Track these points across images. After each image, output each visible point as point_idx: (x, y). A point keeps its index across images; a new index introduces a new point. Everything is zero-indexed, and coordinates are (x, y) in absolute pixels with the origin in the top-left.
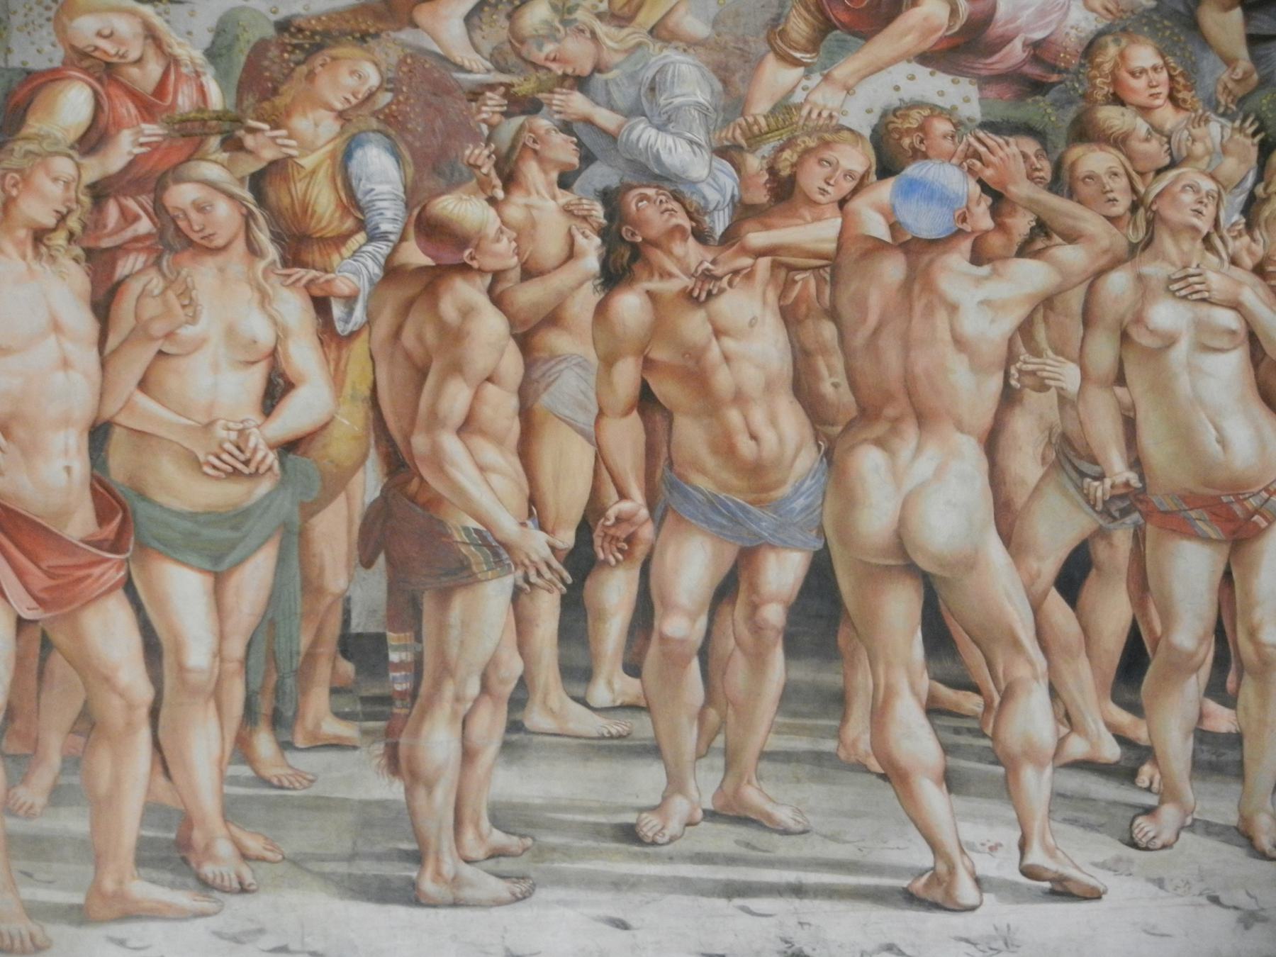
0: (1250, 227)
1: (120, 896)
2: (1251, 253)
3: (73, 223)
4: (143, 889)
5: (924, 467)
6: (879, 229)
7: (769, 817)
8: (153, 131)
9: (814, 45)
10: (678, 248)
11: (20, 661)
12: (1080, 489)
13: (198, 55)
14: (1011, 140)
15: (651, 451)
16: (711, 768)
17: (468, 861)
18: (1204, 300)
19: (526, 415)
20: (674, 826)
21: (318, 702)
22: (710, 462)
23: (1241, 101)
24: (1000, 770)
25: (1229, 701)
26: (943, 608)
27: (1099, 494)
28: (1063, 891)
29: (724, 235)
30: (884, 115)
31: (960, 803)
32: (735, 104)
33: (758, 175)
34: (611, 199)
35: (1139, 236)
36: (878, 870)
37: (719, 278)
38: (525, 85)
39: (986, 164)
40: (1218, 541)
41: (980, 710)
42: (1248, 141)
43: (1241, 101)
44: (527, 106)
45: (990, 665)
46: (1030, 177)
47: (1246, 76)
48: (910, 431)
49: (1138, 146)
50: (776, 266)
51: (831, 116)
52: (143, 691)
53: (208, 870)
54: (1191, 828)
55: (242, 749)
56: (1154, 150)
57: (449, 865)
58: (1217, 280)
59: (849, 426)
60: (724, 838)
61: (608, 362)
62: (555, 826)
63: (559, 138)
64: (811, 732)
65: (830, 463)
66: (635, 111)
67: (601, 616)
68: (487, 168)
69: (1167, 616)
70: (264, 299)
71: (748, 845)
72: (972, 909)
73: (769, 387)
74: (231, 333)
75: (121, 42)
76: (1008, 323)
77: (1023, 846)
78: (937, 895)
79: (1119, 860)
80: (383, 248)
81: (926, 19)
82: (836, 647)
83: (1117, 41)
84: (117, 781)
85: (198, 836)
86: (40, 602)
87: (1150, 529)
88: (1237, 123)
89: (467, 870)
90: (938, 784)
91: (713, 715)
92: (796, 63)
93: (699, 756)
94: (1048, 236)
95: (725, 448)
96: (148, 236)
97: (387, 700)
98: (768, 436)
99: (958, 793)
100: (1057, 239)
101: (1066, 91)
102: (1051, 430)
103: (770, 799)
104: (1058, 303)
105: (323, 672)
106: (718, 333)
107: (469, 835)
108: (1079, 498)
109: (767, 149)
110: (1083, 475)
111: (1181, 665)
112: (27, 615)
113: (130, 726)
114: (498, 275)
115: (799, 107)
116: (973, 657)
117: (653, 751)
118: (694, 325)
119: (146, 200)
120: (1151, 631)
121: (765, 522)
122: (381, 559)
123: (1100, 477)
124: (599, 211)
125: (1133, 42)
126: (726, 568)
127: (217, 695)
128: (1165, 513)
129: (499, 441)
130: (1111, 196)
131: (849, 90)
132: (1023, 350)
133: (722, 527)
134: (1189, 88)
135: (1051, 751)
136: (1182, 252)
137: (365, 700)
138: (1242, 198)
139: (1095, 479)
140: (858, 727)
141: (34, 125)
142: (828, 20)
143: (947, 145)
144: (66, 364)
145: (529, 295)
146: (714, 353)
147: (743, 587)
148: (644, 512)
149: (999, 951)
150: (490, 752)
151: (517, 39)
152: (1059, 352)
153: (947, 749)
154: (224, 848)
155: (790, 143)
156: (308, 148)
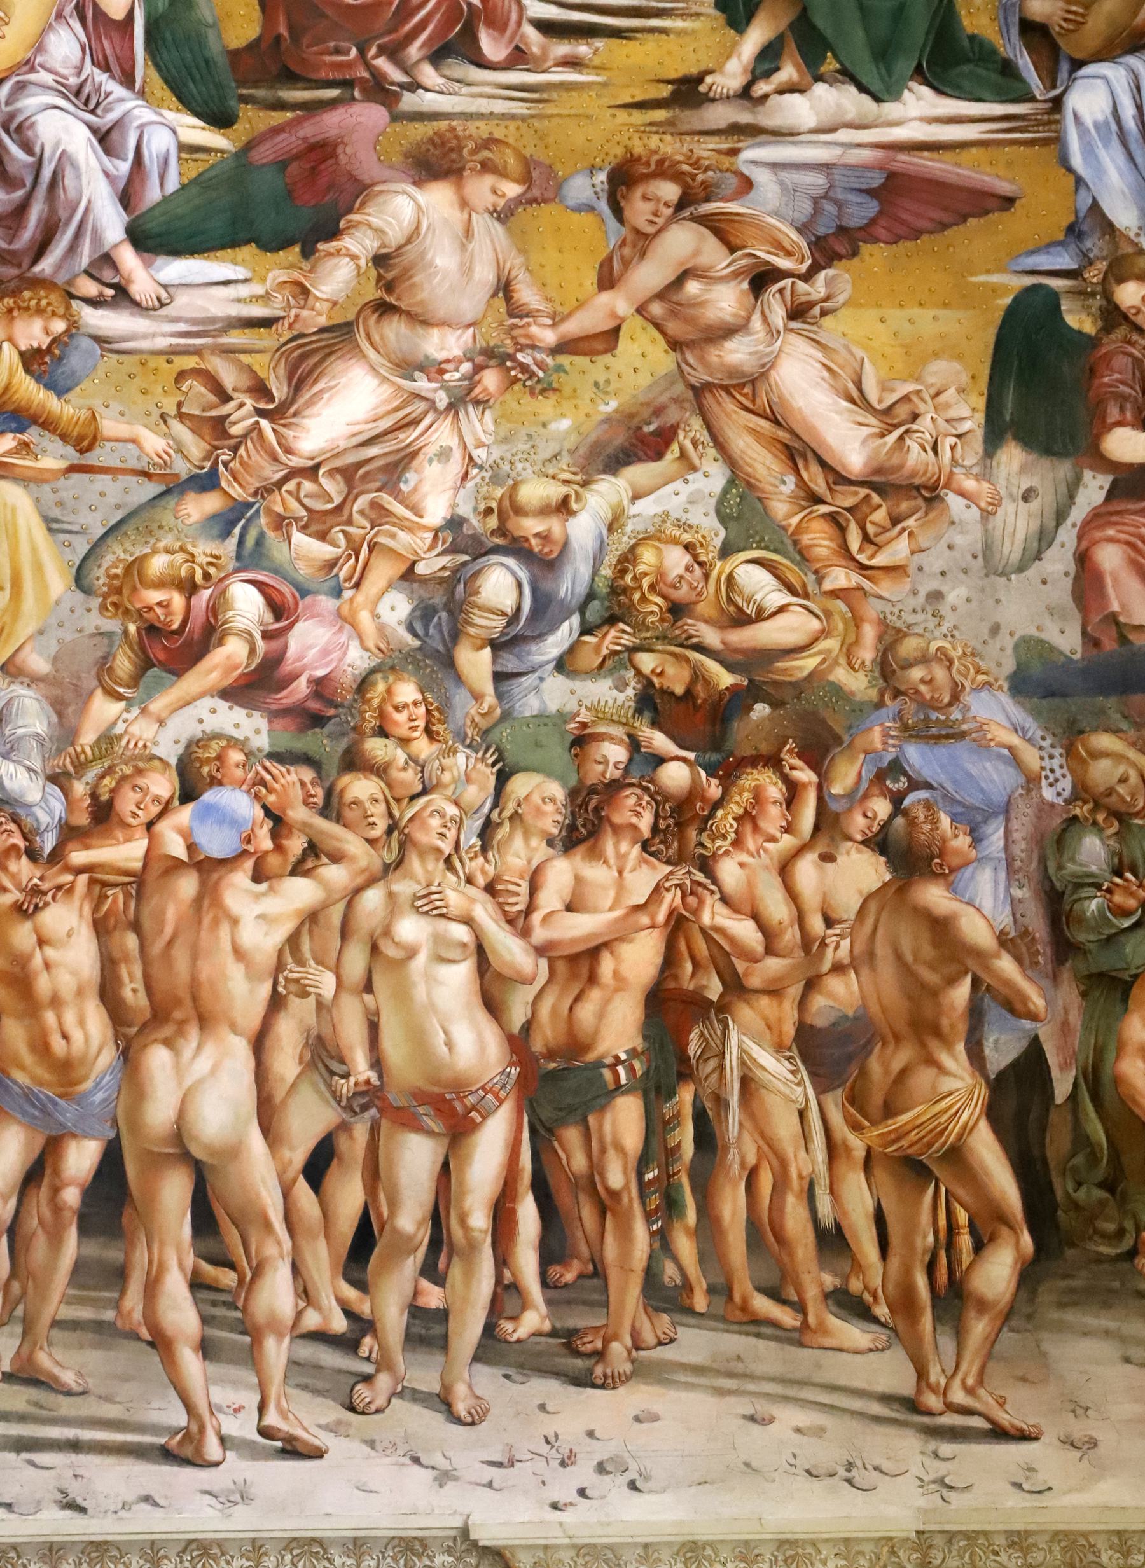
0: (484, 850)
2: (483, 872)
5: (202, 1065)
6: (178, 849)
7: (56, 1379)
9: (135, 681)
12: (329, 1086)
14: (292, 769)
16: (11, 1335)
18: (442, 915)
23: (485, 733)
24: (248, 1339)
26: (210, 1192)
27: (344, 1091)
29: (50, 855)
30: (188, 746)
31: (212, 1368)
33: (81, 800)
35: (391, 857)
36: (141, 1428)
37: (45, 893)
39: (270, 791)
40: (439, 1135)
41: (234, 1284)
42: (489, 770)
46: (306, 803)
47: (491, 710)
48: (193, 1033)
50: (92, 882)
51: (145, 746)
54: (400, 1395)
56: (409, 778)
58: (455, 898)
59: (144, 1026)
60: (18, 1398)
64: (94, 1303)
65: (126, 1060)
69: (393, 1204)
71: (37, 1404)
73: (80, 992)
79: (339, 1422)
81: (228, 658)
82: (120, 1227)
83: (385, 678)
87: (385, 1124)
88: (480, 754)
90: (195, 1350)
91: (16, 1286)
92: (119, 697)
94: (317, 856)
99: (211, 1360)
100: (324, 860)
101: (341, 724)
102: (308, 1031)
103: (57, 1363)
104: (321, 917)
108: (328, 1095)
109: (91, 775)
110: (332, 1073)
111: (404, 1246)
115: (119, 738)
116: (232, 1236)
120: (379, 1215)
121: (68, 1113)
123: (346, 1076)
126: (37, 1151)
128: (398, 1108)
130: (371, 820)
131: (161, 723)
132: (290, 960)
133: (35, 1117)
135: (290, 1323)
136: (427, 871)
138: (480, 823)
139: (342, 1077)
140: (133, 1300)
142: (148, 657)
143: (239, 773)
147: (48, 1171)
149: (236, 1504)
152: (319, 962)
153: (205, 1320)
155: (109, 771)
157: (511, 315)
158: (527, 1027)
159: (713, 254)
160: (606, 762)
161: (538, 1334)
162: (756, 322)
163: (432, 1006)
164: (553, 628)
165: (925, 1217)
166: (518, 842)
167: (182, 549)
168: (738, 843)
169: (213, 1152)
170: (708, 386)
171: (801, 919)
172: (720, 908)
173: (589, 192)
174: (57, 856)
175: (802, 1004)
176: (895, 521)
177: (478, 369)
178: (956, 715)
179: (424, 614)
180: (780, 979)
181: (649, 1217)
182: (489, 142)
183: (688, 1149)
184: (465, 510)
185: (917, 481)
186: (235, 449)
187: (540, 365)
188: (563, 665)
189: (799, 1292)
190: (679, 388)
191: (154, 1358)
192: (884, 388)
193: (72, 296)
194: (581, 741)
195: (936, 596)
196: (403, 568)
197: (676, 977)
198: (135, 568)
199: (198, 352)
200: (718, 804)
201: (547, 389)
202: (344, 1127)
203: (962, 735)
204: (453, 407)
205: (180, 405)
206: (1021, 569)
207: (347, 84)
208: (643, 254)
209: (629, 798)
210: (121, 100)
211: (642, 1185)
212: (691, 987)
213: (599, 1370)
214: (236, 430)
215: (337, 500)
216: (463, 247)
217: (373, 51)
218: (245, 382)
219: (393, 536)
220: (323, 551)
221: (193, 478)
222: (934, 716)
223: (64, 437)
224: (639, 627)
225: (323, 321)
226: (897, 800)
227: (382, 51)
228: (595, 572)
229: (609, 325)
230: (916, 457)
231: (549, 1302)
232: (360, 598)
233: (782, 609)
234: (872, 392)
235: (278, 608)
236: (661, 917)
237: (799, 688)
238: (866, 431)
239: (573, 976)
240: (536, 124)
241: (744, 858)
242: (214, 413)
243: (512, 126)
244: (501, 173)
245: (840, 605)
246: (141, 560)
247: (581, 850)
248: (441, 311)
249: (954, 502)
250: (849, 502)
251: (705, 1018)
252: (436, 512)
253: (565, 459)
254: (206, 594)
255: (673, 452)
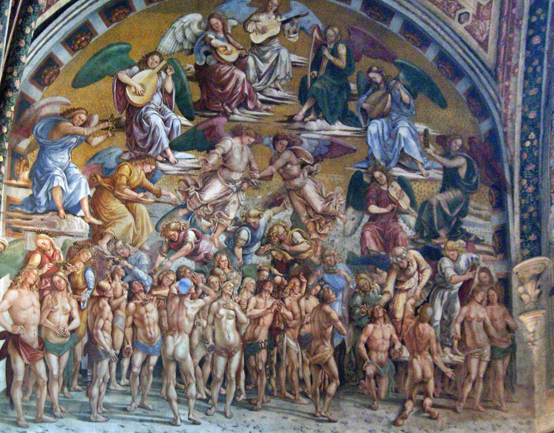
0: (238, 294)
1: (41, 418)
3: (37, 283)
4: (45, 417)
5: (179, 341)
6: (175, 291)
8: (51, 265)
9: (167, 252)
10: (141, 294)
11: (25, 372)
13: (60, 249)
15: (133, 334)
17: (99, 413)
19: (113, 327)
20: (133, 408)
21: (75, 382)
22: (142, 337)
23: (240, 268)
25: (225, 388)
28: (195, 423)
31: (179, 406)
32: (153, 264)
34: (130, 283)
35: (219, 295)
36: (165, 418)
38: (117, 259)
43: (240, 268)
44: (117, 263)
45: (187, 380)
49: (221, 276)
50: (157, 299)
52: (46, 379)
53: (56, 414)
55: (62, 391)
57: (96, 414)
58: (231, 305)
60: (140, 411)
61: (127, 316)
62: (113, 408)
63: (122, 270)
64: (156, 391)
66: (135, 265)
67: (123, 368)
68: (109, 276)
70: (69, 301)
72: (179, 426)
73: (154, 323)
74: (63, 308)
75: (46, 245)
76: (195, 312)
77: (189, 414)
78: (174, 423)
80: (90, 292)
84: (41, 396)
85: (54, 407)
86: (29, 361)
87: (215, 354)
89: (98, 415)
92: (164, 256)
93: (138, 395)
95: (146, 335)
96: (49, 287)
97: (87, 382)
98: (153, 333)
105: (76, 376)
106: (146, 312)
107: (99, 408)
111: (218, 381)
112: (27, 363)
113: (44, 386)
114: (110, 298)
116: (184, 378)
117: (130, 394)
118: (142, 310)
119: (49, 279)
121: (151, 350)
122: (87, 355)
123: (208, 344)
124: (128, 286)
125: (223, 254)
127: (58, 381)
129: (108, 332)
131: (172, 262)
134: (231, 265)
137: (83, 382)
141: (30, 263)
143: (189, 275)
144: (34, 313)
145: (115, 302)
146: (145, 316)
148: (131, 347)
150: (103, 393)
151: (116, 249)
152: (203, 318)
153: (178, 395)
154: (58, 410)
156: (78, 270)
157: (251, 170)
158: (245, 334)
159: (294, 158)
160: (264, 275)
161: (243, 400)
162: (301, 175)
163: (226, 329)
164: (255, 245)
165: (320, 377)
166: (245, 293)
167: (178, 222)
168: (290, 295)
169: (180, 358)
170: (290, 190)
171: (301, 312)
172: (285, 310)
173: (269, 142)
174: (150, 292)
175: (299, 331)
176: (326, 223)
177: (243, 183)
178: (335, 268)
179: (228, 241)
180: (295, 325)
181: (267, 375)
182: (248, 128)
183: (275, 361)
184: (238, 216)
185: (331, 214)
186: (190, 199)
187: (256, 182)
188: (257, 253)
189: (295, 392)
190: (284, 190)
191: (167, 403)
192: (327, 193)
193: (157, 160)
194: (260, 271)
195: (333, 241)
196: (224, 229)
197: (275, 324)
198: (168, 226)
199: (183, 175)
200: (286, 286)
201: (257, 188)
202: (207, 355)
203: (336, 273)
204: (237, 191)
205: (179, 187)
206: (351, 235)
207: (218, 112)
208: (279, 157)
209: (268, 284)
210: (170, 113)
211: (266, 369)
212: (278, 326)
213: (255, 408)
214: (191, 194)
215: (211, 212)
216: (241, 153)
217: (225, 104)
218: (193, 183)
219: (223, 221)
220: (208, 224)
221: (181, 205)
222: (331, 268)
223: (154, 194)
224: (273, 245)
225: (210, 169)
226: (322, 286)
227: (227, 104)
228: (264, 232)
229: (270, 174)
230: (332, 208)
231: (246, 393)
232: (215, 236)
233: (302, 242)
234: (324, 193)
235: (198, 237)
236: (273, 311)
237: (304, 260)
238: (322, 202)
239: (255, 323)
240: (259, 124)
241: (291, 298)
242: (186, 190)
243: (254, 124)
244: (251, 137)
245: (314, 242)
246: (170, 224)
247: (258, 296)
248: (236, 169)
249: (338, 220)
250: (317, 218)
251: (280, 333)
252: (232, 216)
253: (260, 205)
254: (183, 233)
255: (282, 205)
